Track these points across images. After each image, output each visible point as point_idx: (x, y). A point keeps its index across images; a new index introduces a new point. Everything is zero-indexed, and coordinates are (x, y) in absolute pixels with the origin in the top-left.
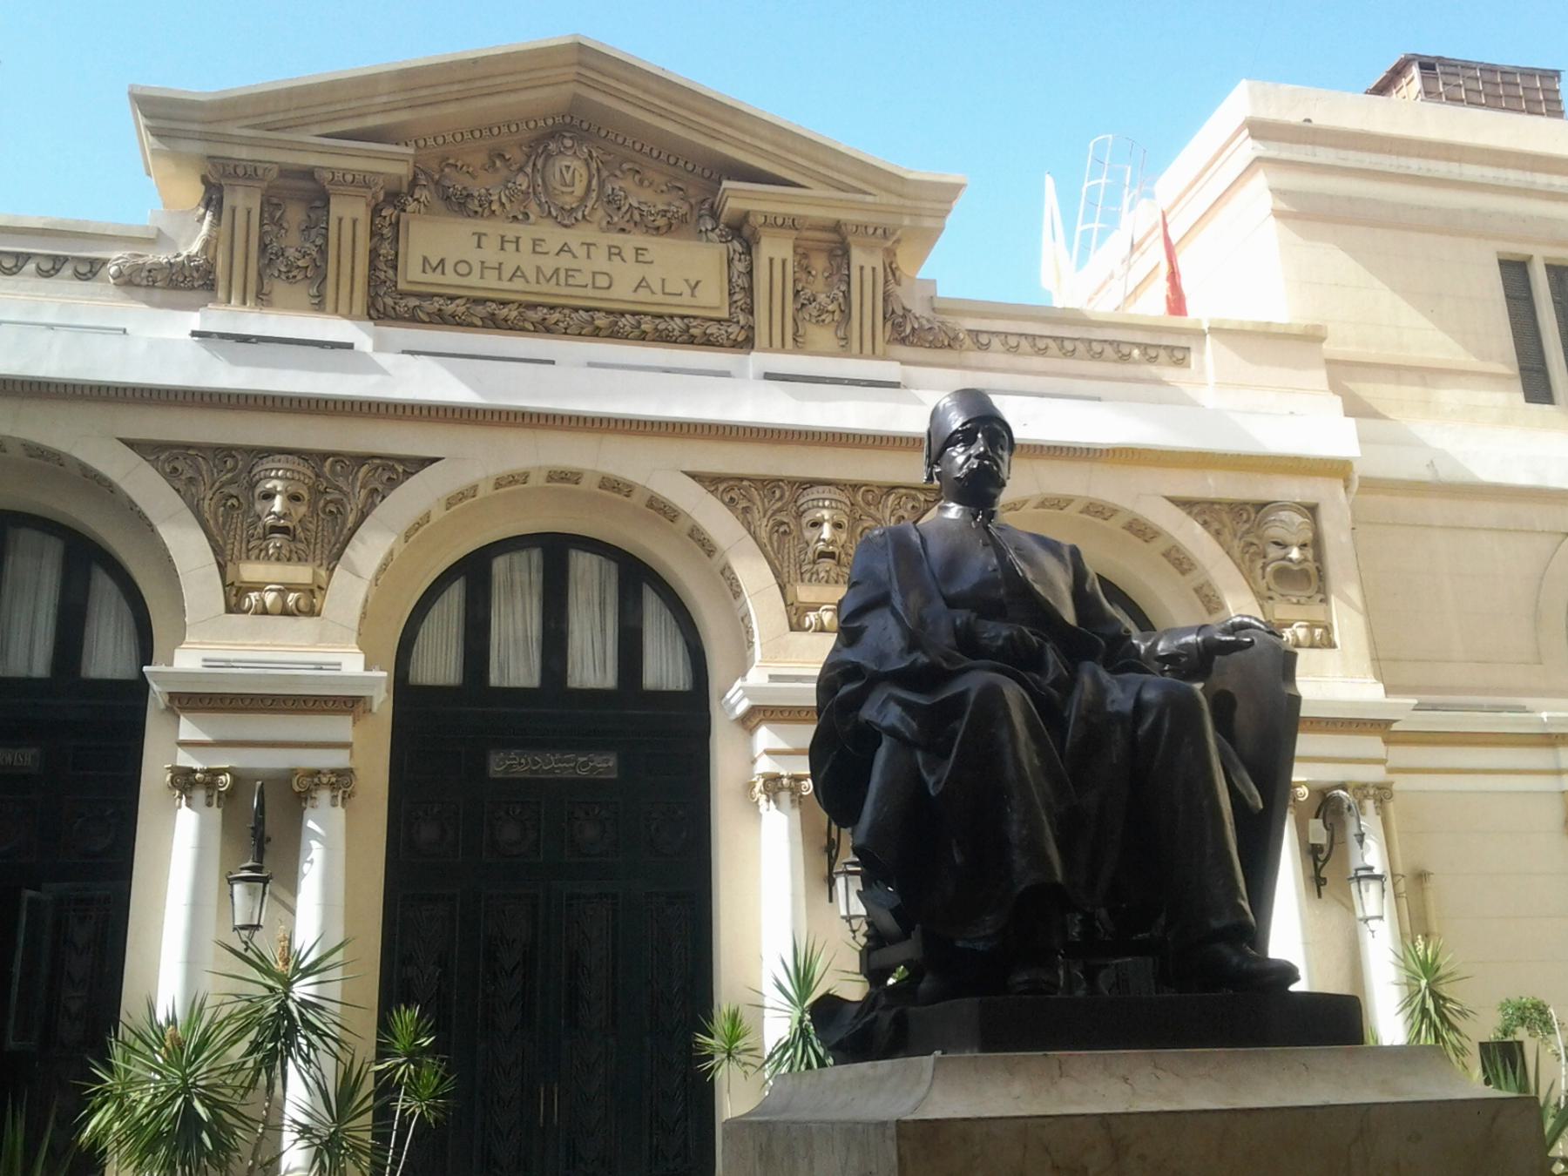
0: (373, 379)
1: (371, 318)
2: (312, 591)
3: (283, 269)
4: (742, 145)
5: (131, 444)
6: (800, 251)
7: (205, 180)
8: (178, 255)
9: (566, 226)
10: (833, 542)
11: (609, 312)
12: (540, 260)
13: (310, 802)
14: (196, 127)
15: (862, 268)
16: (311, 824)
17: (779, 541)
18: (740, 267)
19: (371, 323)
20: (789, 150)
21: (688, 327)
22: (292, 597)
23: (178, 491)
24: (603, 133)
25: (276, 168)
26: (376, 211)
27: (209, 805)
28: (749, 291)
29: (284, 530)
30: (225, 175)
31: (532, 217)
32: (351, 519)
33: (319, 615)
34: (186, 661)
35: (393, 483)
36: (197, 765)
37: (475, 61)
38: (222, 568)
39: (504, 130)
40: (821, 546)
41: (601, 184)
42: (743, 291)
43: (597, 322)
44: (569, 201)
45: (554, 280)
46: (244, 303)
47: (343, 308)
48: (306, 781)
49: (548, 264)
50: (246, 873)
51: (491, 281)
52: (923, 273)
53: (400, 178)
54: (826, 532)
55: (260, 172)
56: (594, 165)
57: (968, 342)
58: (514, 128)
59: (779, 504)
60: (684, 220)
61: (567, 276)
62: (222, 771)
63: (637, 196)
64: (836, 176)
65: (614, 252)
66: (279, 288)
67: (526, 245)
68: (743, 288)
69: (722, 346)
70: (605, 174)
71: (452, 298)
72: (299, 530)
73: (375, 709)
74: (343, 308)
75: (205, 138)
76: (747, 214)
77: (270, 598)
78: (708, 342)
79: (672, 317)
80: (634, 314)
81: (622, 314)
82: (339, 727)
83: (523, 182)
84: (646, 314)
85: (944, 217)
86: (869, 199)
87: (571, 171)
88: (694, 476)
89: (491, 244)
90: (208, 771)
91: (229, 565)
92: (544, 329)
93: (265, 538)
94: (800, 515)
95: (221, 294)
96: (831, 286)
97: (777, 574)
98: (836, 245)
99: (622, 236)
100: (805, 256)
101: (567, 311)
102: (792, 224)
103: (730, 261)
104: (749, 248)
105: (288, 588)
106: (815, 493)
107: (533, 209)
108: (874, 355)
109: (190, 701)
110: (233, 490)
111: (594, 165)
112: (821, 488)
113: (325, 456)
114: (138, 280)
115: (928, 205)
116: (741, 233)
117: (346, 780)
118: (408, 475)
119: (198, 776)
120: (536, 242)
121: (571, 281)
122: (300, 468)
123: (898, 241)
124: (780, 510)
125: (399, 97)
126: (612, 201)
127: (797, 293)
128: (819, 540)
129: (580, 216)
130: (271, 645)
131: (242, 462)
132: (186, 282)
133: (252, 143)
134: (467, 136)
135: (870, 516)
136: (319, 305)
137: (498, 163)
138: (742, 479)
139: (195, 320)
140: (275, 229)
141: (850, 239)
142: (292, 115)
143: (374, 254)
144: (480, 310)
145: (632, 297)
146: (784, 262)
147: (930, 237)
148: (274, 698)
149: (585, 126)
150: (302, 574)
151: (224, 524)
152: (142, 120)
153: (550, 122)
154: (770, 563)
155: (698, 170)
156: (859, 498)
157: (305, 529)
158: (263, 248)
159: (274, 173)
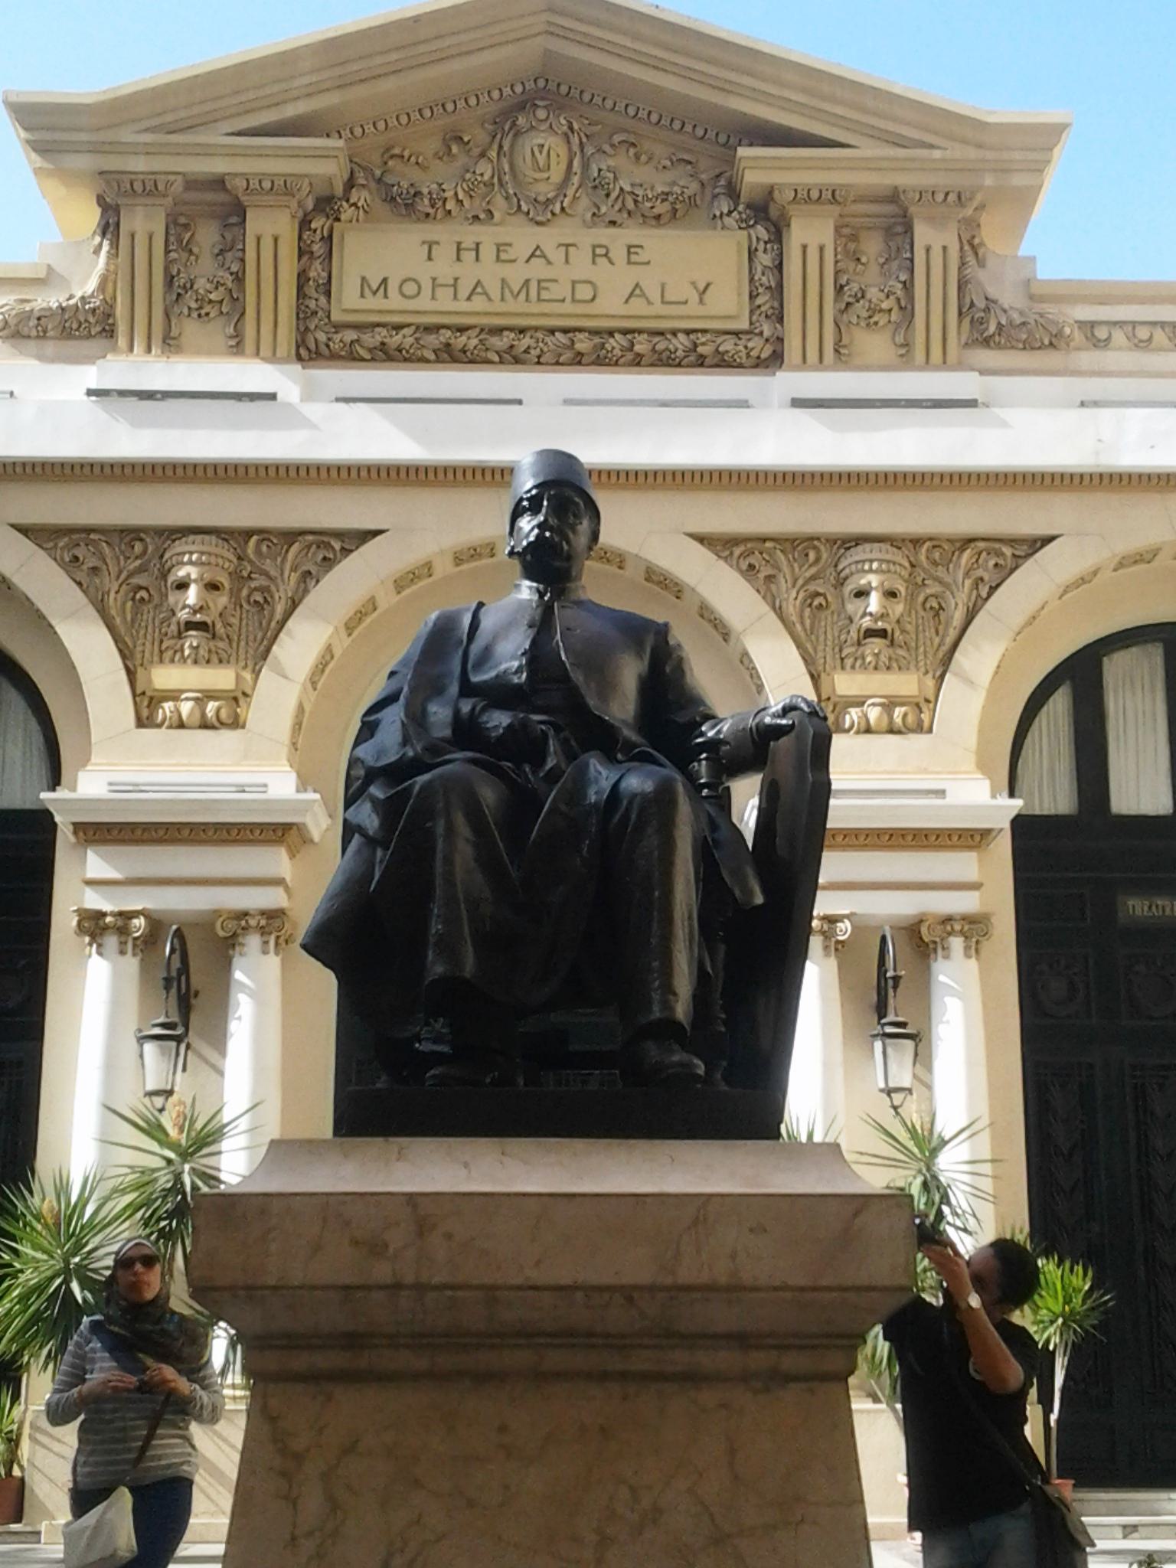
1: (299, 358)
2: (236, 699)
3: (194, 305)
4: (767, 98)
5: (24, 530)
6: (846, 231)
7: (100, 200)
8: (71, 297)
9: (538, 223)
10: (883, 616)
11: (595, 332)
12: (506, 271)
14: (84, 137)
15: (928, 250)
17: (813, 617)
18: (765, 259)
19: (298, 367)
20: (824, 98)
21: (695, 345)
22: (211, 707)
23: (79, 584)
24: (587, 97)
25: (180, 178)
26: (305, 224)
28: (778, 291)
29: (202, 626)
30: (121, 193)
31: (497, 215)
33: (243, 727)
34: (93, 784)
35: (328, 563)
36: (107, 907)
37: (416, 19)
38: (131, 674)
39: (461, 104)
40: (867, 622)
41: (586, 166)
42: (769, 292)
43: (578, 346)
44: (545, 191)
45: (523, 295)
46: (149, 350)
47: (265, 350)
49: (516, 275)
50: (158, 1031)
51: (445, 301)
52: (1024, 251)
53: (330, 181)
54: (874, 603)
55: (161, 187)
56: (575, 140)
57: (1078, 337)
58: (473, 101)
59: (813, 570)
60: (692, 202)
61: (539, 289)
62: (135, 914)
63: (631, 174)
64: (891, 127)
65: (600, 253)
66: (190, 329)
67: (488, 252)
68: (769, 288)
69: (740, 366)
70: (590, 150)
71: (398, 327)
72: (219, 625)
73: (316, 837)
74: (265, 350)
75: (96, 149)
76: (771, 190)
77: (186, 708)
78: (723, 363)
79: (674, 333)
80: (625, 332)
81: (611, 334)
83: (485, 169)
84: (640, 332)
85: (1041, 171)
86: (937, 154)
87: (545, 151)
88: (701, 539)
89: (445, 252)
90: (121, 914)
91: (140, 670)
92: (513, 359)
93: (180, 636)
94: (841, 583)
95: (122, 341)
96: (885, 275)
98: (896, 219)
99: (612, 230)
100: (854, 238)
101: (539, 335)
102: (833, 196)
103: (752, 253)
104: (778, 232)
105: (209, 695)
107: (499, 205)
108: (945, 365)
109: (99, 833)
111: (575, 140)
112: (867, 546)
113: (248, 533)
114: (25, 331)
115: (1017, 155)
116: (766, 215)
117: (277, 923)
118: (346, 552)
119: (108, 919)
120: (499, 248)
121: (545, 295)
122: (218, 551)
123: (982, 207)
124: (813, 578)
125: (326, 74)
126: (599, 186)
127: (839, 289)
128: (864, 614)
129: (557, 209)
130: (222, 764)
131: (148, 547)
132: (84, 328)
133: (149, 151)
134: (415, 116)
136: (237, 347)
137: (455, 149)
138: (764, 540)
139: (92, 375)
140: (185, 255)
141: (912, 210)
142: (196, 110)
143: (302, 278)
144: (432, 340)
145: (623, 310)
146: (822, 249)
147: (1025, 200)
148: (192, 827)
149: (564, 89)
150: (223, 678)
151: (133, 621)
152: (23, 134)
153: (519, 89)
154: (799, 646)
155: (711, 134)
156: (923, 558)
158: (170, 280)
159: (178, 186)
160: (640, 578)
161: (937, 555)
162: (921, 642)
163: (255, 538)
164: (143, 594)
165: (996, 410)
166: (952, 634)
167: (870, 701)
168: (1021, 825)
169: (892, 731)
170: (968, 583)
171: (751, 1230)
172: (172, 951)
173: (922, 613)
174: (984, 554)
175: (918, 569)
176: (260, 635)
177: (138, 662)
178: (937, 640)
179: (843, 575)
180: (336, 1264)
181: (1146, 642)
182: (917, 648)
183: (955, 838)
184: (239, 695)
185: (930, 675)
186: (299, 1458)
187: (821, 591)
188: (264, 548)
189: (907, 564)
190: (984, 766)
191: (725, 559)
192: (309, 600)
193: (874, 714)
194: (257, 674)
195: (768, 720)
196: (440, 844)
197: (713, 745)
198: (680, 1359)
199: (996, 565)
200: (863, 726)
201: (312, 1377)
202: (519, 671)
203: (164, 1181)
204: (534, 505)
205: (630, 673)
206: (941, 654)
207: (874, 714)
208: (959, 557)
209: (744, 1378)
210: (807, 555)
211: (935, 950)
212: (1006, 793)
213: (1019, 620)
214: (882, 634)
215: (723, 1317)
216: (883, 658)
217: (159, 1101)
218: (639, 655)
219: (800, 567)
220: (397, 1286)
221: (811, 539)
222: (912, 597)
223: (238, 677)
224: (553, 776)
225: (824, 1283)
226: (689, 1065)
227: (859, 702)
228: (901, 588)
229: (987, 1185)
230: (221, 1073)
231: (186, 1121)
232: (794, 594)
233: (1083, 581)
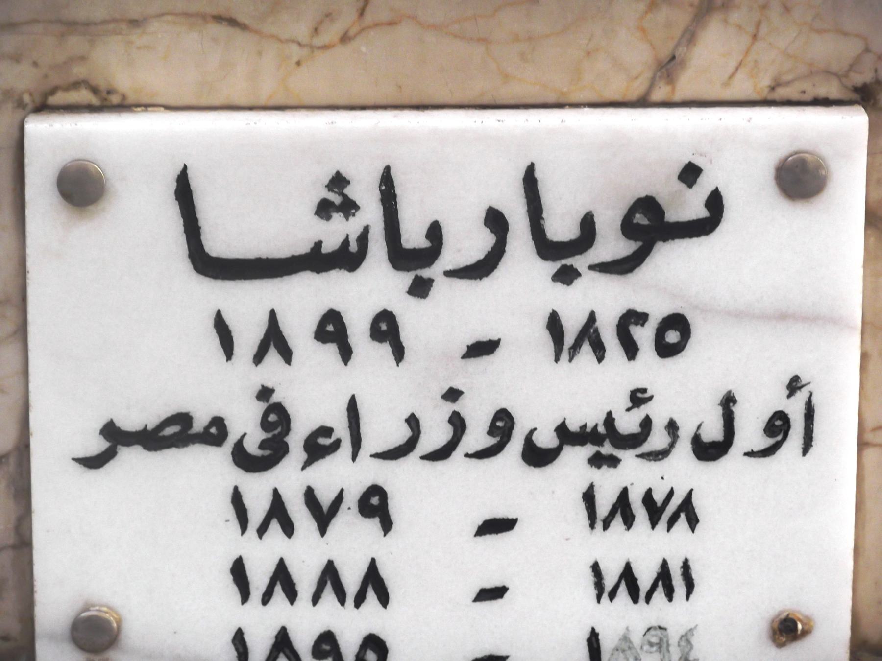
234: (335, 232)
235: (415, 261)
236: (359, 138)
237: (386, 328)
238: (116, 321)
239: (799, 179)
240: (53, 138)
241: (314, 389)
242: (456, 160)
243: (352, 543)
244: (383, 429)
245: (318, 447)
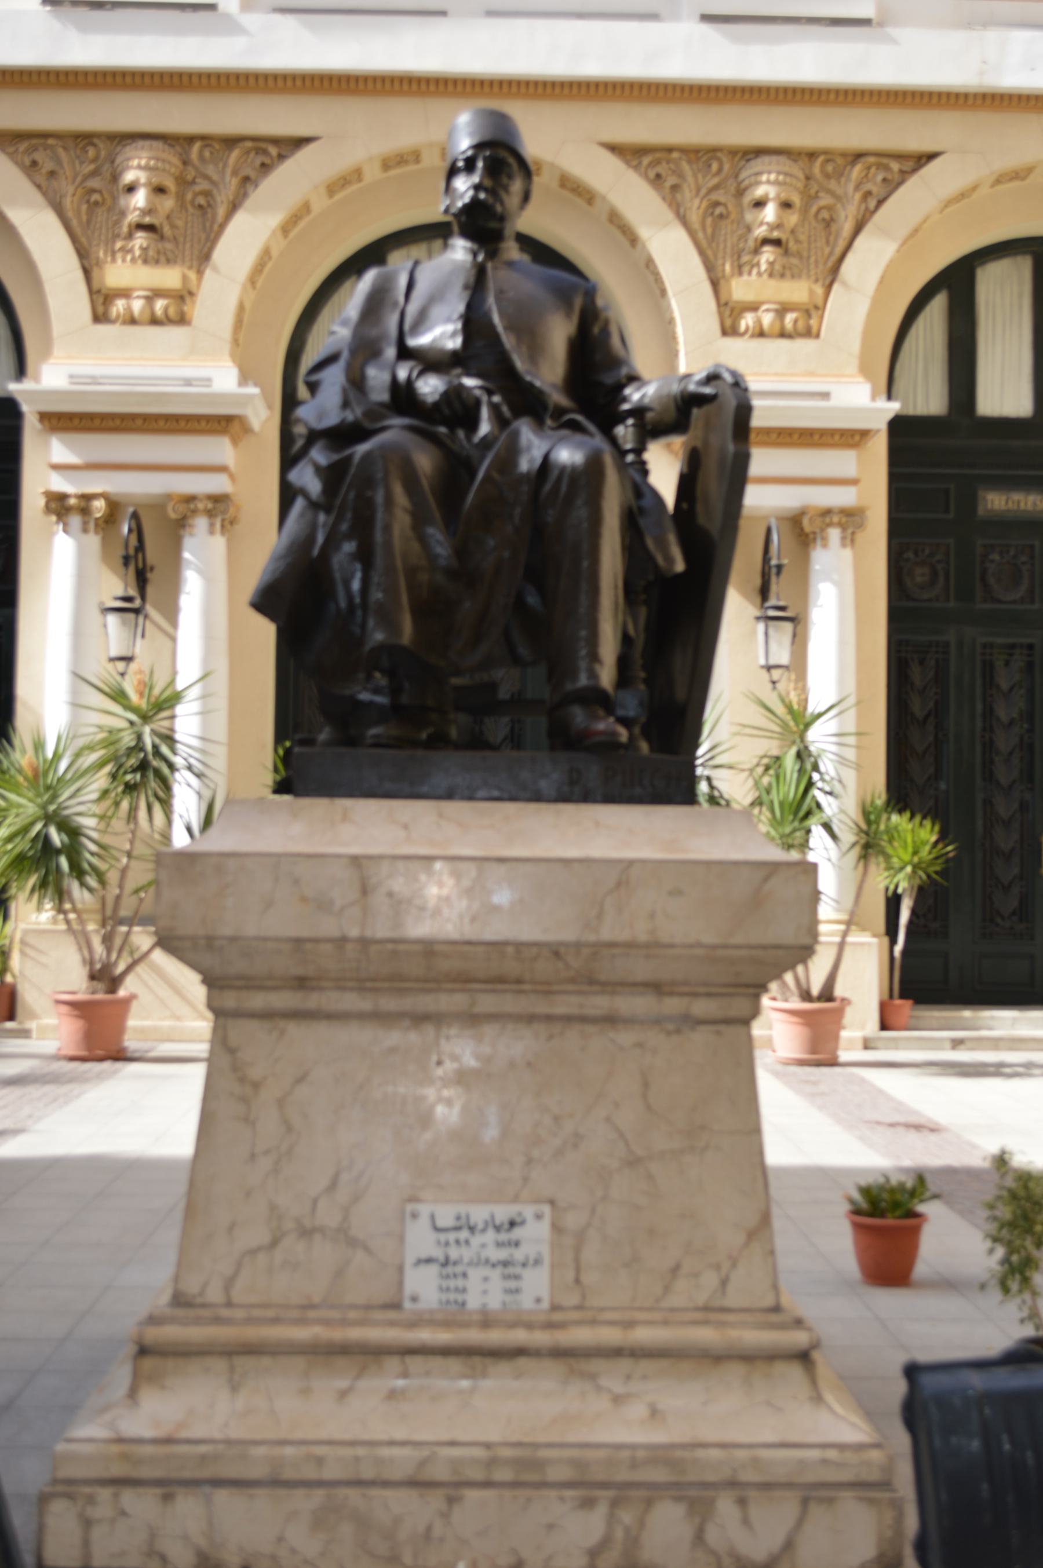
0: (239, 42)
10: (779, 226)
13: (188, 529)
16: (186, 555)
17: (715, 227)
22: (160, 305)
23: (39, 187)
27: (85, 530)
29: (150, 228)
32: (221, 211)
35: (265, 168)
38: (87, 273)
48: (182, 508)
54: (770, 213)
77: (137, 306)
82: (220, 449)
88: (614, 148)
94: (740, 193)
97: (710, 267)
106: (758, 164)
109: (63, 421)
110: (94, 183)
113: (190, 139)
117: (221, 506)
118: (281, 157)
124: (716, 188)
128: (761, 224)
135: (829, 192)
138: (670, 150)
150: (170, 277)
151: (89, 222)
154: (701, 252)
156: (817, 169)
157: (173, 227)
160: (555, 184)
161: (830, 168)
162: (813, 252)
163: (197, 146)
164: (95, 197)
165: (890, 30)
166: (841, 244)
167: (764, 307)
168: (899, 426)
169: (783, 335)
170: (858, 196)
171: (671, 893)
172: (130, 530)
173: (814, 223)
174: (873, 170)
175: (812, 182)
176: (203, 236)
177: (94, 262)
178: (827, 250)
179: (743, 185)
180: (284, 921)
181: (1016, 254)
182: (809, 257)
183: (837, 437)
184: (185, 293)
185: (820, 283)
186: (256, 1086)
187: (722, 199)
188: (207, 154)
189: (801, 176)
190: (865, 370)
191: (636, 168)
192: (249, 203)
193: (767, 319)
194: (200, 273)
195: (692, 387)
196: (380, 515)
197: (639, 412)
198: (599, 1004)
199: (884, 180)
200: (757, 330)
201: (267, 1015)
202: (453, 335)
203: (128, 739)
204: (470, 165)
205: (559, 332)
206: (830, 264)
207: (767, 319)
208: (851, 170)
209: (657, 1021)
210: (710, 166)
211: (815, 540)
212: (884, 396)
213: (905, 232)
214: (777, 243)
215: (642, 970)
216: (777, 267)
217: (121, 666)
218: (568, 314)
219: (704, 177)
220: (341, 941)
221: (713, 152)
222: (805, 210)
223: (185, 278)
224: (486, 443)
225: (734, 941)
226: (615, 734)
227: (754, 307)
228: (796, 199)
229: (851, 754)
230: (173, 639)
231: (145, 687)
232: (697, 202)
233: (963, 195)
234: (458, 1224)
235: (472, 1229)
236: (463, 1209)
237: (467, 1242)
238: (420, 1240)
239: (539, 1217)
240: (410, 1207)
241: (454, 1253)
242: (479, 1214)
243: (460, 1283)
244: (466, 1260)
245: (455, 1263)
